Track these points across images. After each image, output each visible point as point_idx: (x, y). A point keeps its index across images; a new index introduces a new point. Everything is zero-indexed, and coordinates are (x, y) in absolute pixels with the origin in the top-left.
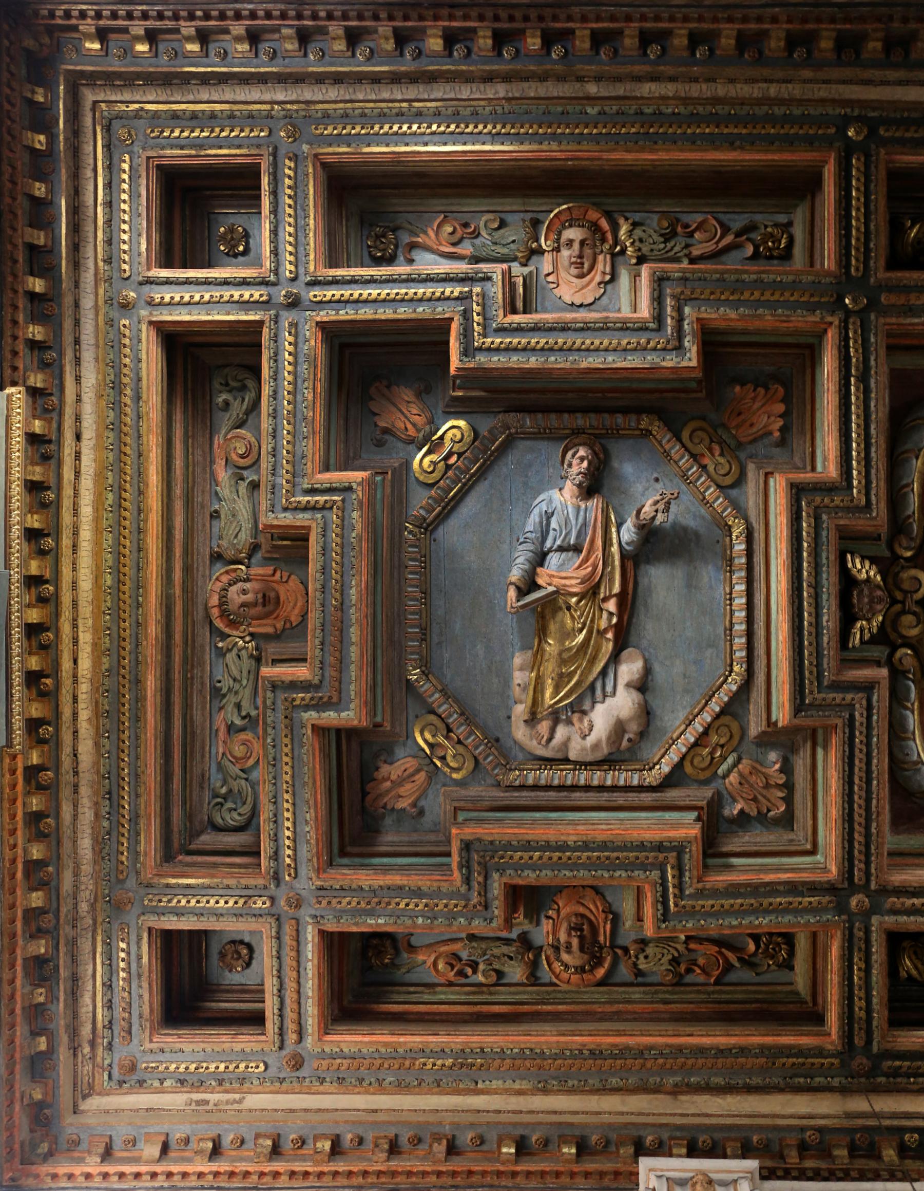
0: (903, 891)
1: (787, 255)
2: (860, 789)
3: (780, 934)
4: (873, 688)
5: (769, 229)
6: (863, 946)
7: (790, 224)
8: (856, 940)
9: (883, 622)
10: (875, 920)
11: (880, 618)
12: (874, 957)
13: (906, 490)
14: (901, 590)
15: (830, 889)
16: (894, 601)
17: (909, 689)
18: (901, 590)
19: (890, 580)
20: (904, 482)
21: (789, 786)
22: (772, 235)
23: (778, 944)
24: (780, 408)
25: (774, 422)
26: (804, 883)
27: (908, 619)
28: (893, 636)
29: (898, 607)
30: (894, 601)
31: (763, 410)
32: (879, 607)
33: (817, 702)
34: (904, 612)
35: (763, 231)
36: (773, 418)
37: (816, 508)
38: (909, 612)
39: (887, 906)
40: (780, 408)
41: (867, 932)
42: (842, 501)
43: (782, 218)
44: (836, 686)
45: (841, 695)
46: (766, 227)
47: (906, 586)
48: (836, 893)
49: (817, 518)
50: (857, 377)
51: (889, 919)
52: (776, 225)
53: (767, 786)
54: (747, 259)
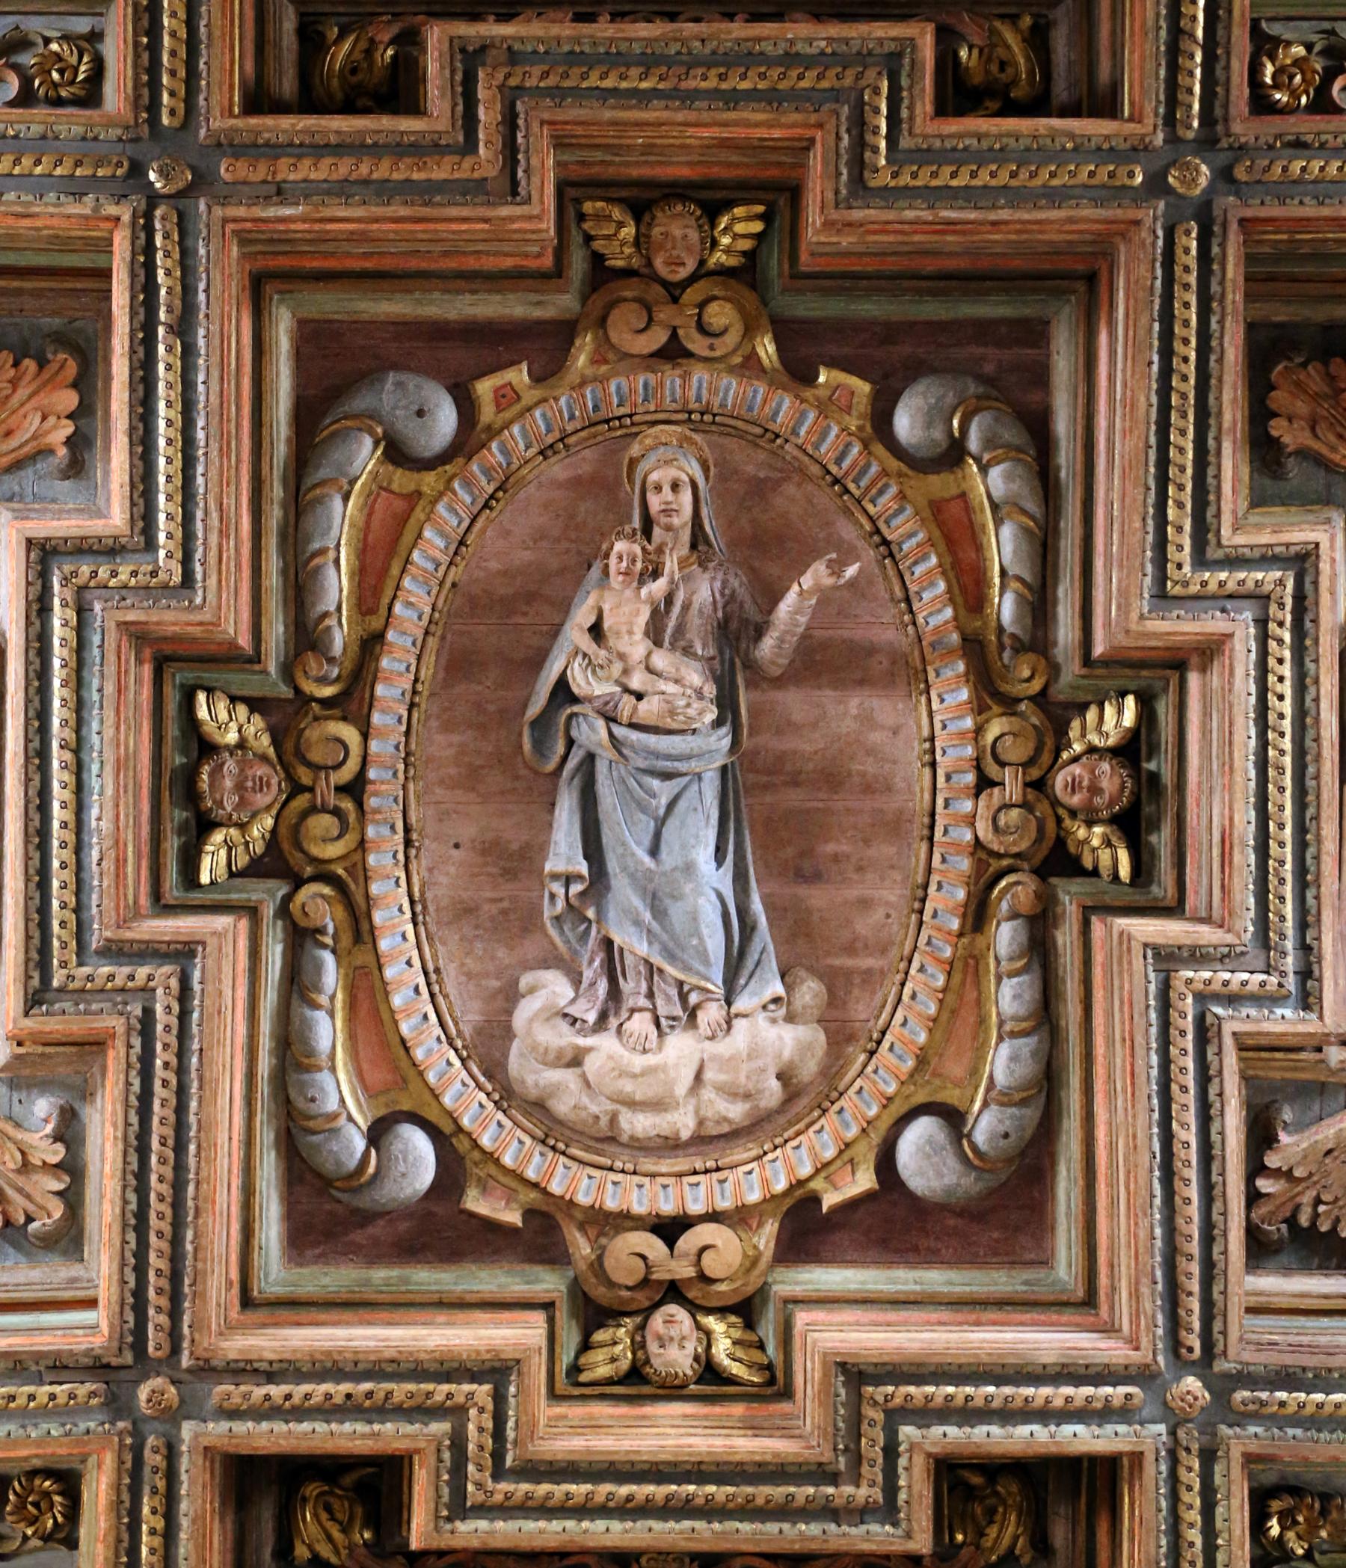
0: (244, 1370)
1: (91, 95)
2: (163, 1161)
3: (48, 1473)
4: (192, 954)
5: (54, 47)
6: (161, 1484)
7: (95, 37)
8: (147, 1471)
9: (274, 831)
10: (187, 1430)
11: (269, 822)
12: (183, 1506)
13: (316, 561)
14: (309, 764)
15: (97, 1367)
16: (297, 789)
17: (319, 967)
18: (309, 764)
19: (289, 746)
20: (316, 545)
21: (73, 1168)
22: (58, 57)
23: (47, 1494)
24: (69, 400)
25: (55, 427)
26: (38, 1356)
27: (324, 823)
28: (295, 858)
29: (301, 801)
30: (297, 789)
31: (33, 403)
32: (262, 800)
33: (76, 985)
34: (313, 810)
35: (41, 50)
36: (52, 420)
37: (81, 589)
38: (324, 810)
39: (214, 1400)
40: (69, 400)
41: (171, 1453)
42: (134, 574)
43: (82, 25)
44: (116, 951)
45: (126, 970)
46: (47, 41)
47: (316, 756)
48: (111, 1374)
49: (82, 611)
50: (170, 329)
51: (217, 1430)
52: (66, 38)
53: (26, 1167)
54: (11, 104)
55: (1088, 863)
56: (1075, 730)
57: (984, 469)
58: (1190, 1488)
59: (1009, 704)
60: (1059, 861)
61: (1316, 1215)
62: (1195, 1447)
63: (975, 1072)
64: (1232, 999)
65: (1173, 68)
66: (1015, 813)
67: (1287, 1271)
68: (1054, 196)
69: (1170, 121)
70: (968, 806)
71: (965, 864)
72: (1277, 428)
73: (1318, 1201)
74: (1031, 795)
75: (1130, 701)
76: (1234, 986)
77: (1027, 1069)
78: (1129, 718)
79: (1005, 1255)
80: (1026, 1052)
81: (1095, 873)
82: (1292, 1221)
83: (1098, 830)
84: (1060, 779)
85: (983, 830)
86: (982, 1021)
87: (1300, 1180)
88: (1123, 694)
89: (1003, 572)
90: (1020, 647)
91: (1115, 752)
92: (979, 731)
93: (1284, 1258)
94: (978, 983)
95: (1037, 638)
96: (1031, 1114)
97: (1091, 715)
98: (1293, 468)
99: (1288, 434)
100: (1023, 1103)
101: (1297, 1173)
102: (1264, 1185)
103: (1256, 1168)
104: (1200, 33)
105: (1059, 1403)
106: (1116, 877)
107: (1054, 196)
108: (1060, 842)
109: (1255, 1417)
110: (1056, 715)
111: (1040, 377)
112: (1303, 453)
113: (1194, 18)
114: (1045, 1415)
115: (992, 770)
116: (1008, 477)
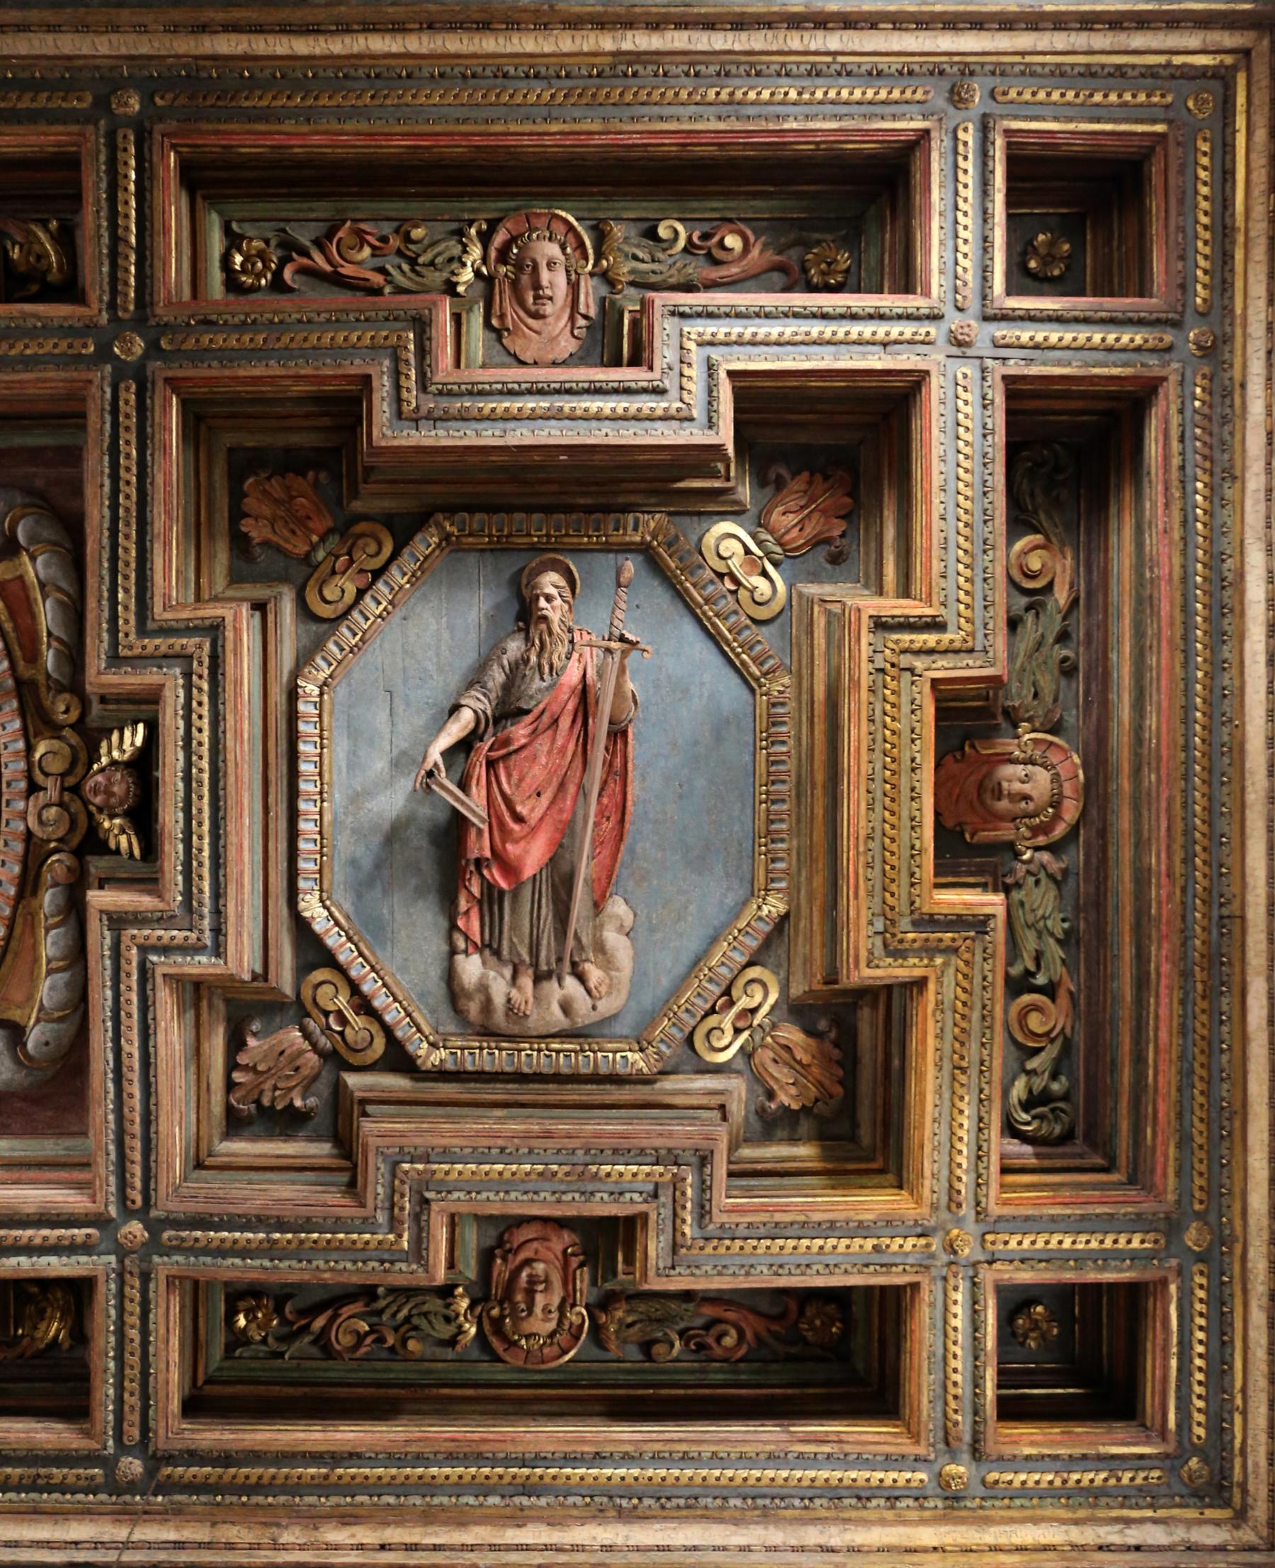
55: (112, 845)
56: (103, 750)
57: (33, 559)
58: (132, 1301)
59: (54, 729)
60: (91, 843)
61: (274, 1099)
62: (136, 1270)
63: (30, 997)
64: (165, 950)
65: (114, 266)
66: (54, 810)
67: (255, 1138)
68: (28, 363)
69: (112, 306)
70: (21, 805)
71: (19, 847)
72: (246, 526)
73: (275, 1088)
74: (67, 796)
75: (141, 727)
76: (166, 940)
77: (61, 995)
78: (139, 741)
79: (57, 1130)
80: (61, 983)
81: (117, 851)
82: (258, 1102)
83: (117, 821)
84: (90, 783)
85: (32, 821)
86: (36, 960)
87: (263, 1073)
88: (135, 723)
89: (49, 634)
90: (61, 689)
91: (128, 764)
92: (30, 749)
93: (256, 1129)
94: (34, 934)
95: (74, 683)
96: (68, 1029)
97: (115, 737)
98: (262, 556)
99: (255, 531)
100: (60, 1020)
101: (260, 1068)
102: (238, 1076)
103: (231, 1065)
104: (133, 240)
105: (38, 1241)
106: (131, 855)
107: (28, 363)
108: (93, 828)
109: (178, 1249)
110: (90, 738)
111: (77, 489)
112: (266, 544)
113: (127, 229)
114: (29, 1250)
115: (39, 778)
116: (47, 565)
